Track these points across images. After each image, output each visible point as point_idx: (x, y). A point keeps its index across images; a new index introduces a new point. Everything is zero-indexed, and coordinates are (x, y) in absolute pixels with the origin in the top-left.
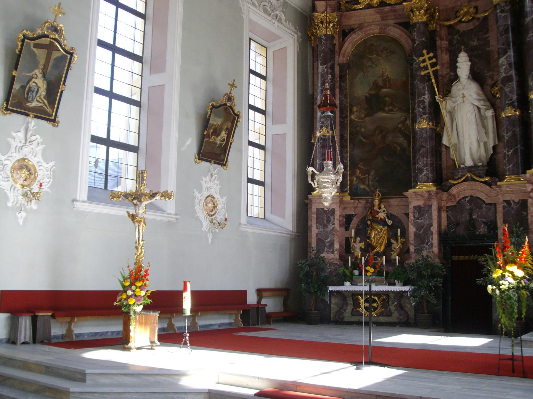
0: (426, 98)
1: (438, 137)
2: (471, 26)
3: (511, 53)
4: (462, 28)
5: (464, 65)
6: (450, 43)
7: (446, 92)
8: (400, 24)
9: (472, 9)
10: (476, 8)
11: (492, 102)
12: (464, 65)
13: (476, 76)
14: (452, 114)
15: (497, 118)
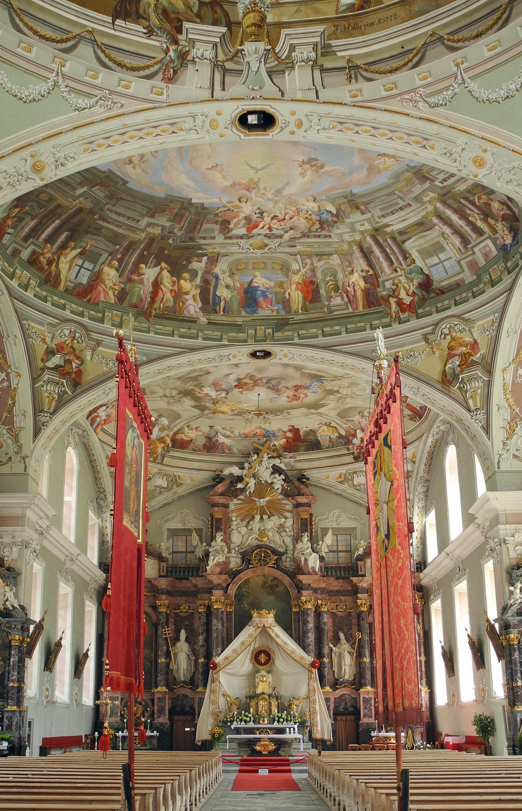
0: (165, 648)
1: (168, 664)
2: (186, 615)
3: (204, 635)
4: (182, 614)
5: (183, 634)
6: (176, 620)
7: (174, 645)
8: (151, 606)
9: (187, 607)
10: (189, 606)
11: (194, 651)
12: (183, 634)
13: (187, 640)
14: (176, 654)
15: (196, 661)
